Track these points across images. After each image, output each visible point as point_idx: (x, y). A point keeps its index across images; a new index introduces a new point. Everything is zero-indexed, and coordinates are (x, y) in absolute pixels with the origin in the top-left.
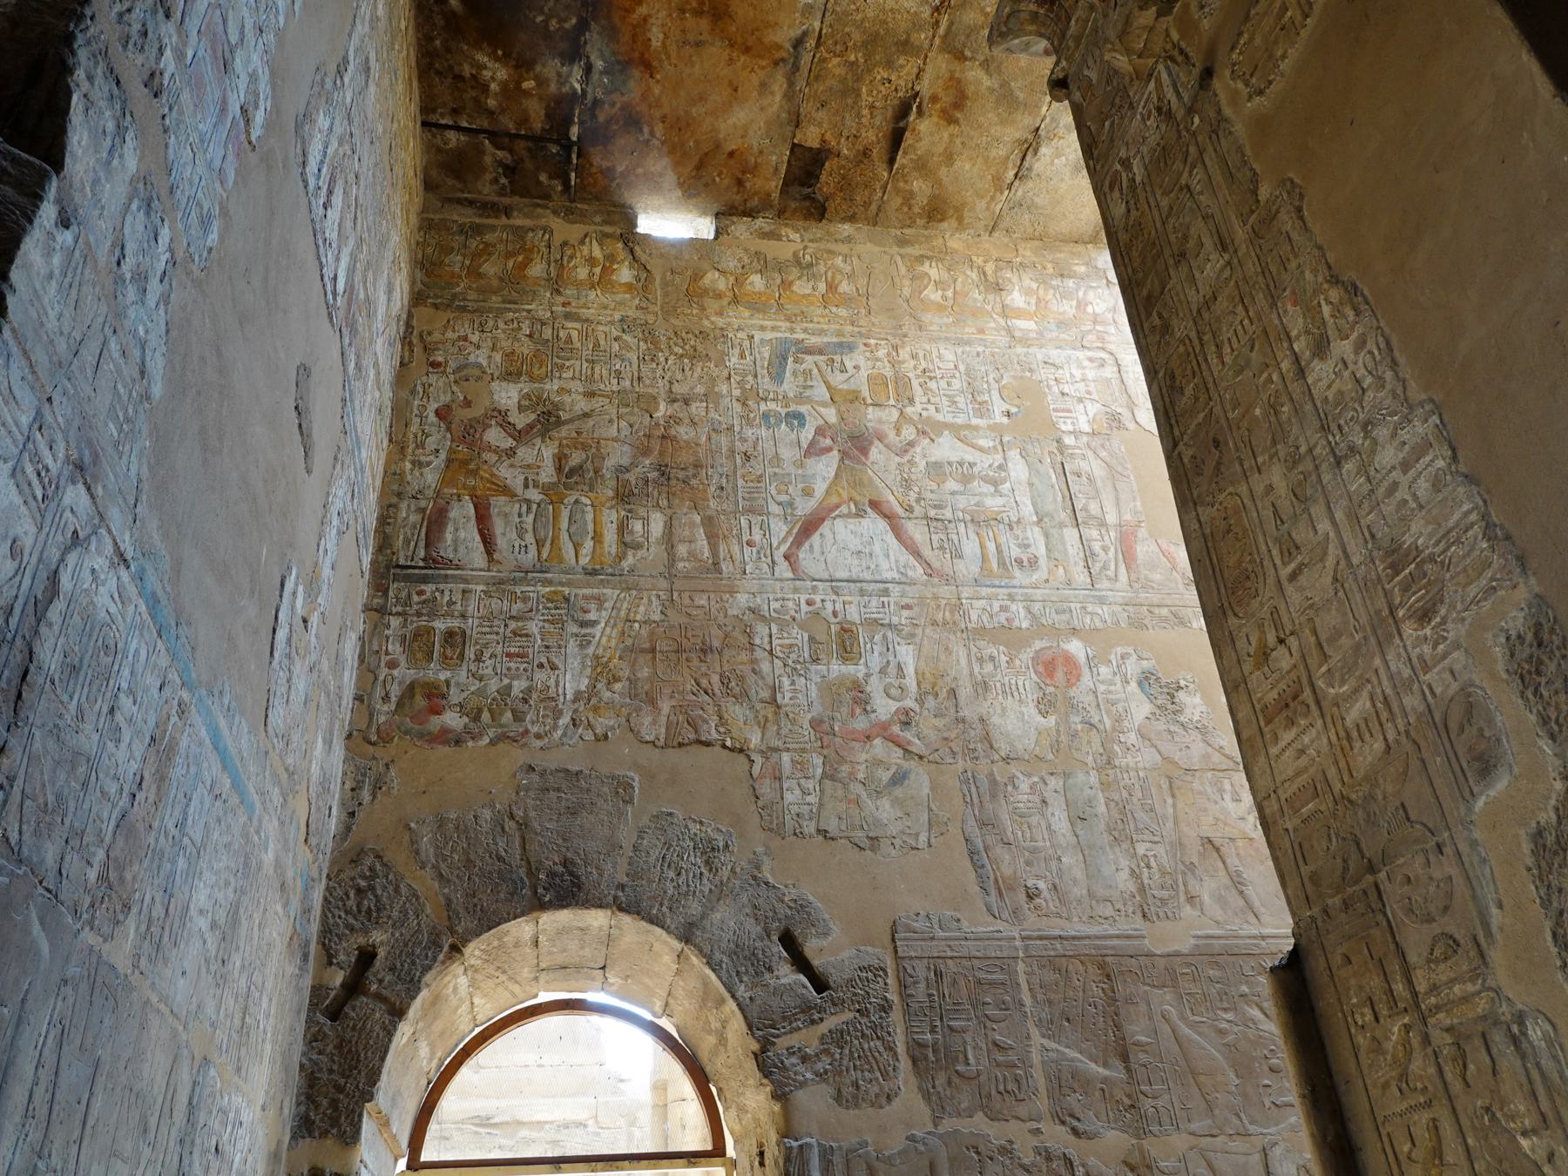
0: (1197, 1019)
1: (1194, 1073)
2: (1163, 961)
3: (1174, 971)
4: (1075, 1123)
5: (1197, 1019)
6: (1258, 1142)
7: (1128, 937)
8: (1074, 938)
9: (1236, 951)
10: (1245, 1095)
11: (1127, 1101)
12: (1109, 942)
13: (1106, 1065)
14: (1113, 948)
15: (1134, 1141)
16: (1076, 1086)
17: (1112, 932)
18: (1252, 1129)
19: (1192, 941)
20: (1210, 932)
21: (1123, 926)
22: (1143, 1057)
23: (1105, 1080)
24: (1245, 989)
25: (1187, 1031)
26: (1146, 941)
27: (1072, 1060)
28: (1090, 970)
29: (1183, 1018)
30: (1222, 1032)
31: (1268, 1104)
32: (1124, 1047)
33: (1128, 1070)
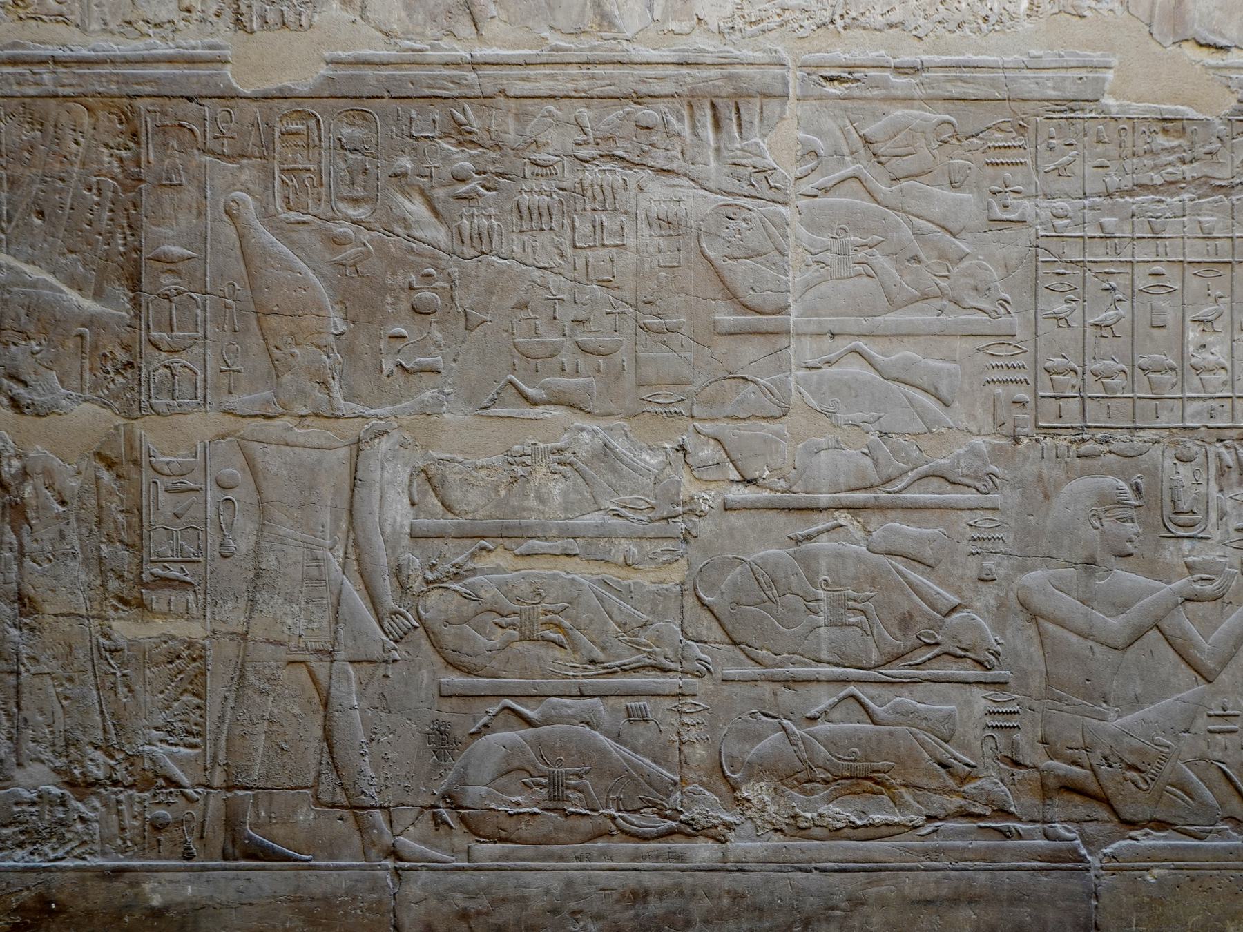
0: (293, 216)
1: (261, 312)
2: (253, 107)
3: (274, 127)
4: (18, 390)
5: (293, 216)
6: (352, 429)
7: (192, 61)
8: (81, 62)
9: (411, 90)
10: (350, 351)
11: (122, 356)
12: (149, 71)
13: (98, 295)
14: (156, 80)
15: (120, 421)
16: (31, 329)
17: (163, 50)
18: (343, 406)
19: (324, 70)
20: (366, 52)
21: (191, 40)
22: (168, 282)
23: (92, 321)
24: (406, 162)
25: (268, 237)
26: (228, 70)
27: (34, 285)
28: (103, 122)
29: (267, 215)
30: (337, 242)
31: (388, 365)
32: (137, 263)
33: (136, 303)
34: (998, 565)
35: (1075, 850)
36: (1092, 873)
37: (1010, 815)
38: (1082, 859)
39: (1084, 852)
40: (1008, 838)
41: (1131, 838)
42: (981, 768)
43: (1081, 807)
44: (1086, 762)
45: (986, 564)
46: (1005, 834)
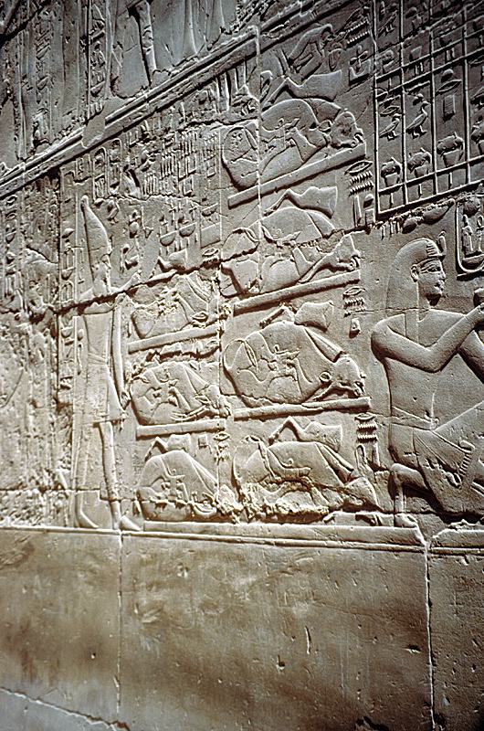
34: (360, 320)
35: (413, 535)
36: (425, 556)
37: (375, 508)
38: (419, 544)
39: (420, 537)
40: (372, 525)
41: (451, 528)
42: (356, 470)
43: (421, 503)
44: (415, 463)
45: (354, 320)
46: (367, 520)
